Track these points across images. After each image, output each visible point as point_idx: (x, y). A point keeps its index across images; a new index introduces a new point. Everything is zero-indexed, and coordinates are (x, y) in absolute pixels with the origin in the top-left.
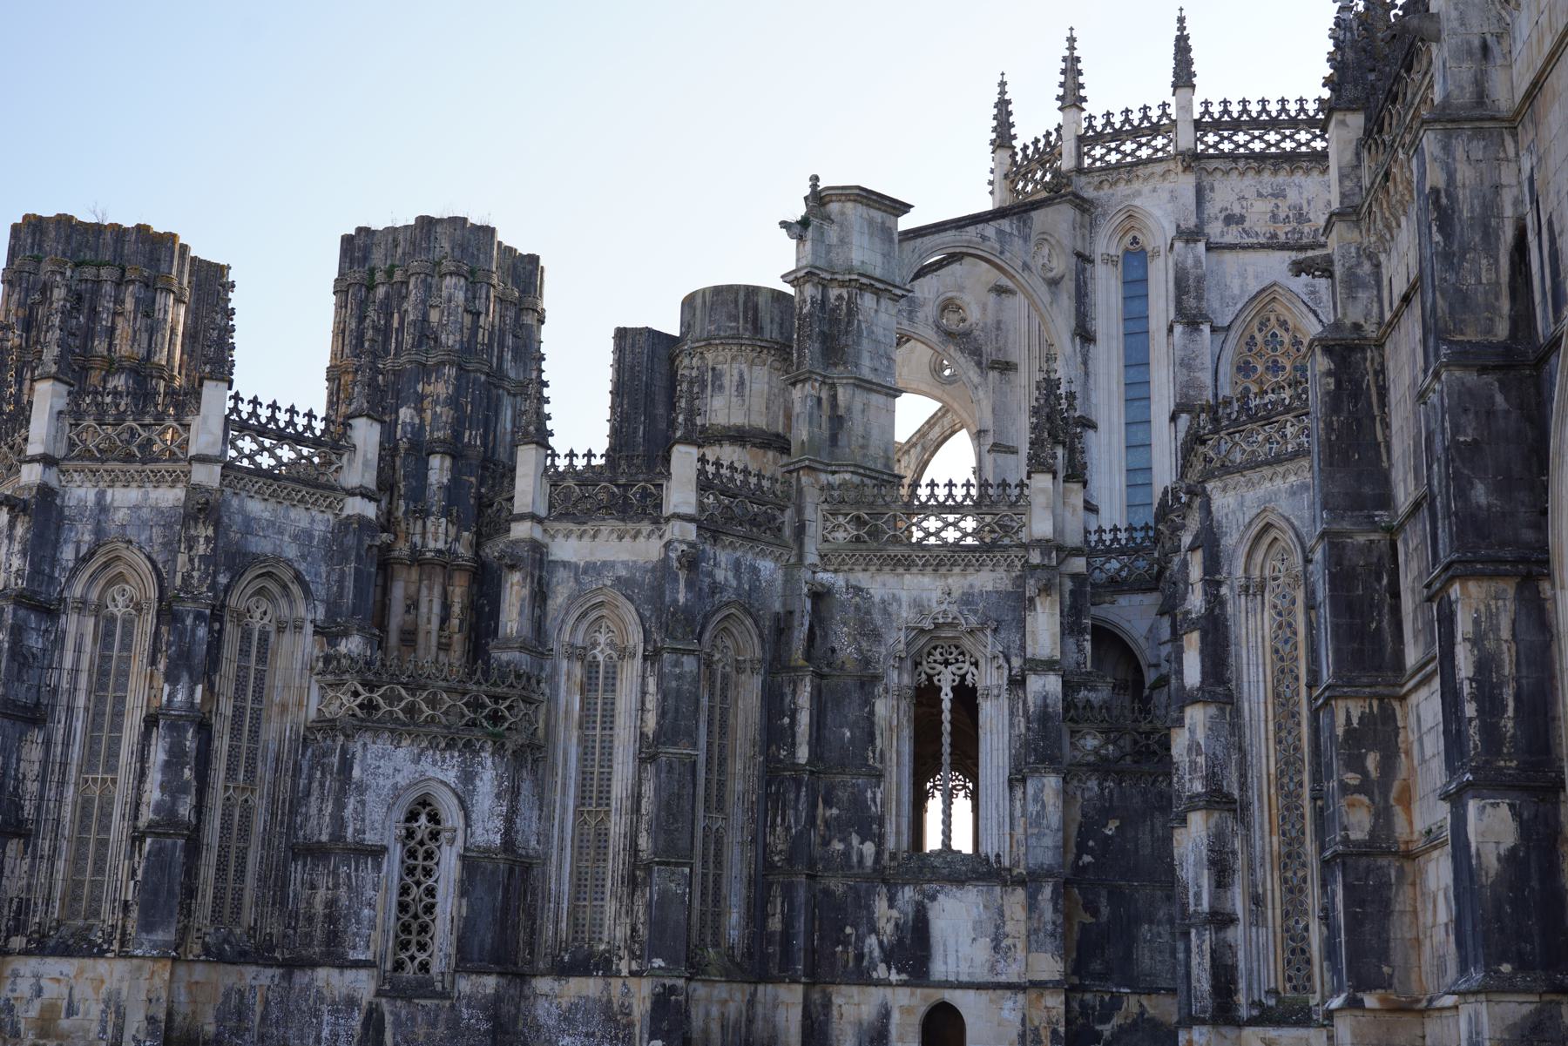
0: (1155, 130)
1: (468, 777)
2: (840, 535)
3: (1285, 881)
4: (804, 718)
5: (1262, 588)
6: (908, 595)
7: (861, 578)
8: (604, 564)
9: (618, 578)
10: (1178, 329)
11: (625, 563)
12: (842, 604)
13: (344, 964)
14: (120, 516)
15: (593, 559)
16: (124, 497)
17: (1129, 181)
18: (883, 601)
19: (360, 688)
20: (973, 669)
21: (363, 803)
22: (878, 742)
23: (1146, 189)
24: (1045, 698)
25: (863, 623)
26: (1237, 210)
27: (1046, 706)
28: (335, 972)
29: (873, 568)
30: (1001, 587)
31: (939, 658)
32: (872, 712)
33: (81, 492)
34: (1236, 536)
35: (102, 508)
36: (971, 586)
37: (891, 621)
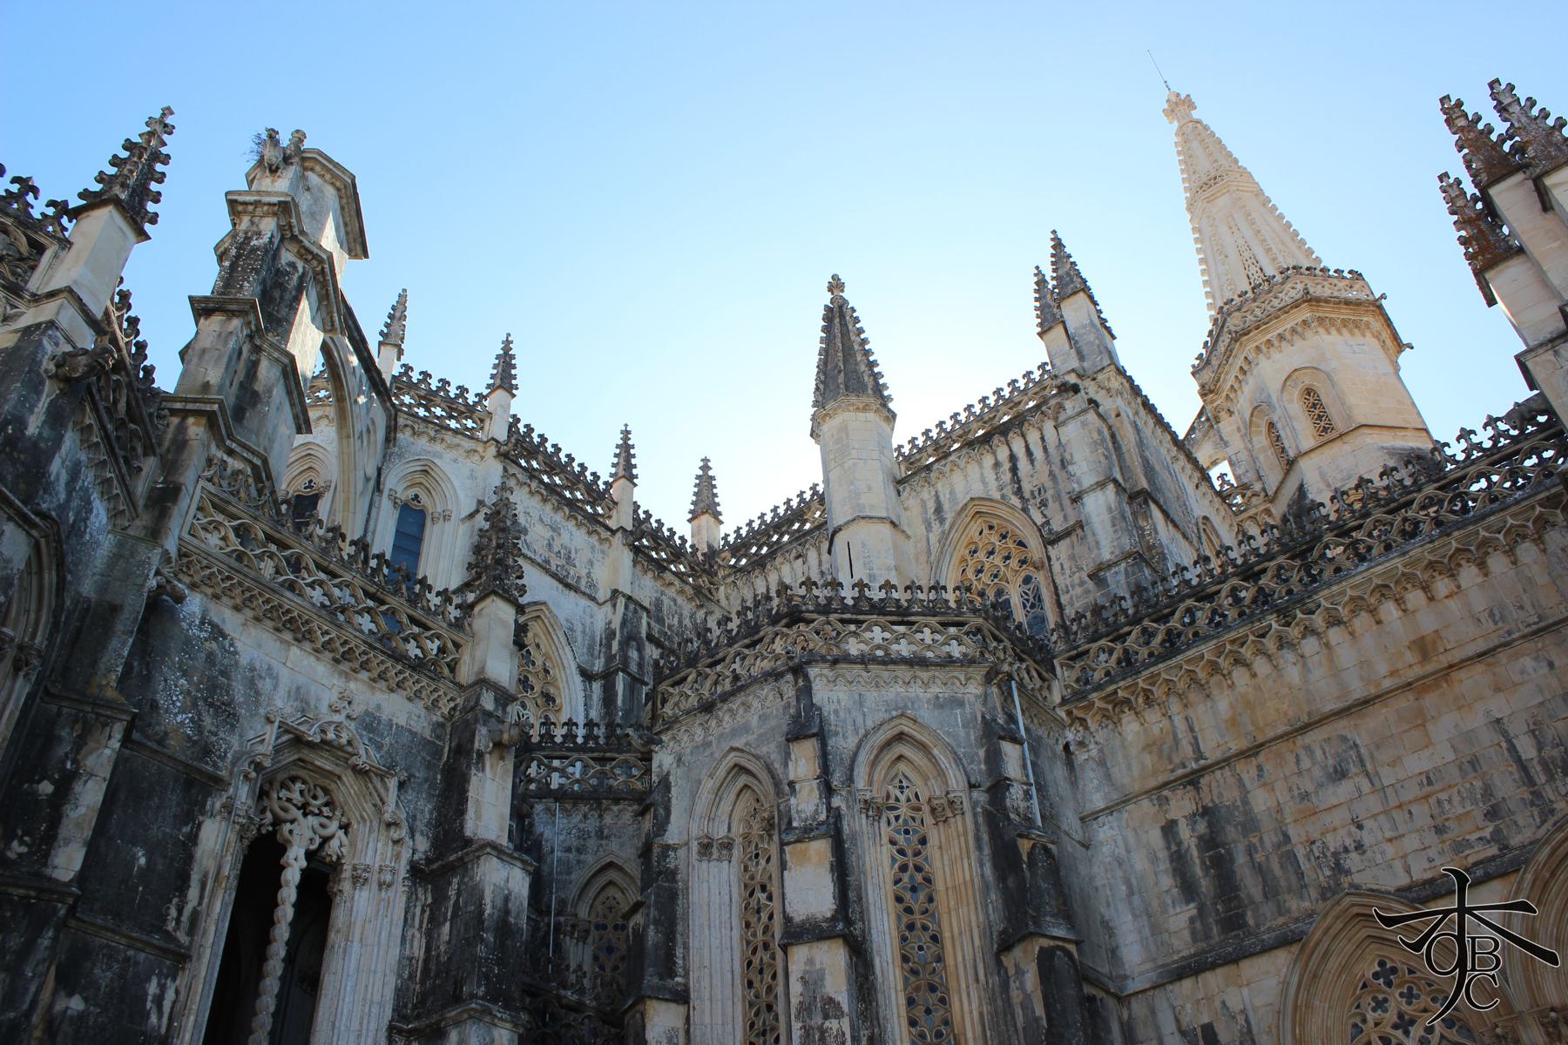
2: (213, 540)
4: (90, 795)
5: (879, 811)
6: (295, 680)
7: (230, 620)
12: (188, 641)
17: (433, 439)
18: (253, 669)
20: (341, 833)
22: (193, 894)
23: (449, 455)
24: (507, 899)
25: (213, 687)
27: (507, 912)
29: (249, 613)
30: (417, 728)
31: (296, 797)
32: (193, 838)
34: (852, 742)
36: (379, 707)
37: (257, 704)
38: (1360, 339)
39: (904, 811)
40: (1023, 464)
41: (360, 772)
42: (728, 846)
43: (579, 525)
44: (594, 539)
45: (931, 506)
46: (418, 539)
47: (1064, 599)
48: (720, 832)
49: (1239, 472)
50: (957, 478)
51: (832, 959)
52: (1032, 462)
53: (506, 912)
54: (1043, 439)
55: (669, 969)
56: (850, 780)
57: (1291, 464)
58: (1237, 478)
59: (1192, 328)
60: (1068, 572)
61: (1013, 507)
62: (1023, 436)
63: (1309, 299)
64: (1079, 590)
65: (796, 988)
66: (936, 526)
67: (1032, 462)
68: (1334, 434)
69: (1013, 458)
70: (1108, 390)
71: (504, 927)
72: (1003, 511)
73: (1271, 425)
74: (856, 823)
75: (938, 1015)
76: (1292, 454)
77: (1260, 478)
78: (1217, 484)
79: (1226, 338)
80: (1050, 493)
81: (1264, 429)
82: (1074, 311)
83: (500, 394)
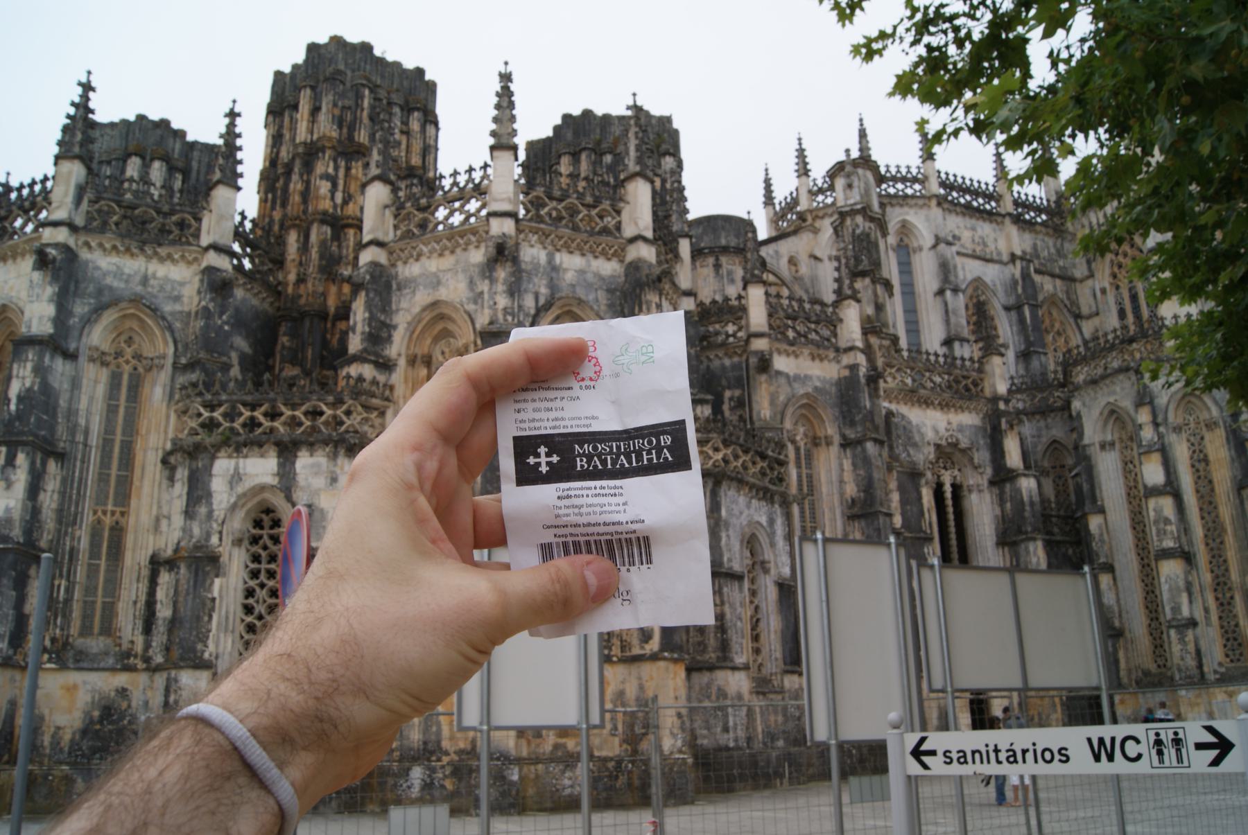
0: (915, 180)
1: (771, 522)
3: (1217, 599)
5: (1180, 429)
8: (806, 376)
9: (816, 388)
10: (948, 293)
11: (818, 378)
13: (734, 668)
14: (569, 277)
15: (798, 372)
16: (571, 263)
19: (721, 446)
21: (728, 536)
22: (927, 515)
23: (912, 211)
26: (957, 233)
28: (729, 673)
33: (534, 251)
35: (554, 268)
39: (1192, 426)
41: (963, 451)
42: (1112, 444)
43: (984, 220)
44: (994, 225)
46: (909, 264)
48: (1109, 438)
51: (1167, 505)
53: (1031, 497)
55: (1094, 499)
56: (1166, 419)
65: (1152, 514)
71: (1032, 504)
74: (1172, 438)
75: (1213, 515)
83: (929, 162)
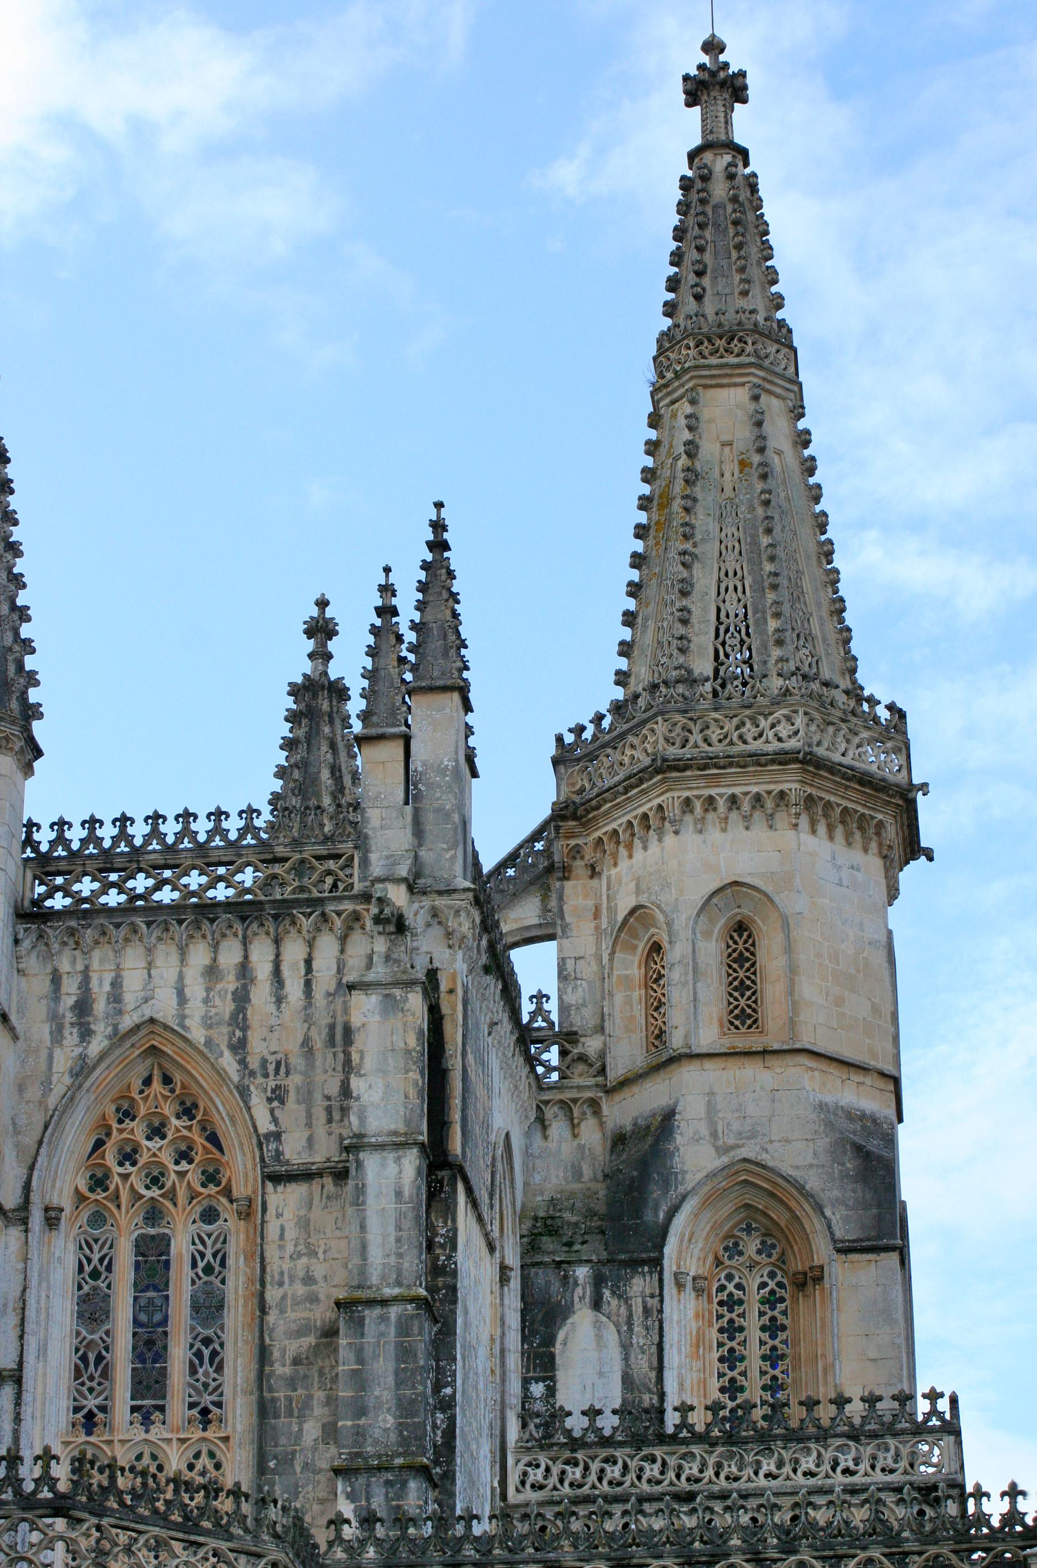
38: (857, 855)
40: (261, 994)
45: (71, 988)
47: (272, 1294)
49: (571, 998)
50: (133, 959)
52: (279, 1000)
54: (308, 962)
57: (664, 1059)
58: (563, 1008)
59: (589, 691)
60: (290, 1248)
61: (221, 1075)
62: (277, 942)
63: (809, 762)
64: (300, 1290)
66: (71, 1036)
67: (279, 1000)
68: (755, 1042)
69: (244, 970)
70: (449, 935)
72: (201, 1073)
73: (656, 948)
76: (676, 1041)
77: (601, 1029)
78: (527, 1008)
79: (636, 754)
80: (294, 1081)
81: (642, 946)
82: (429, 720)
